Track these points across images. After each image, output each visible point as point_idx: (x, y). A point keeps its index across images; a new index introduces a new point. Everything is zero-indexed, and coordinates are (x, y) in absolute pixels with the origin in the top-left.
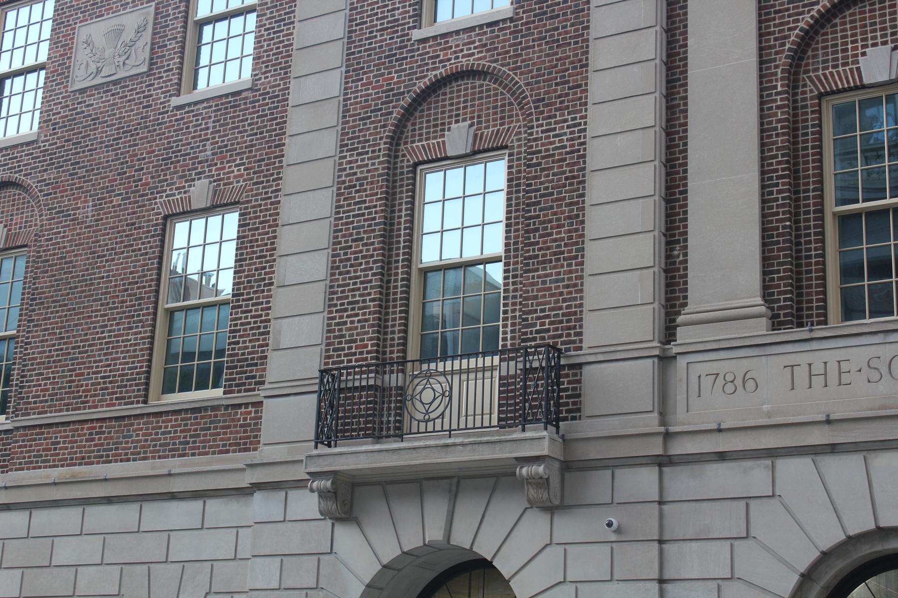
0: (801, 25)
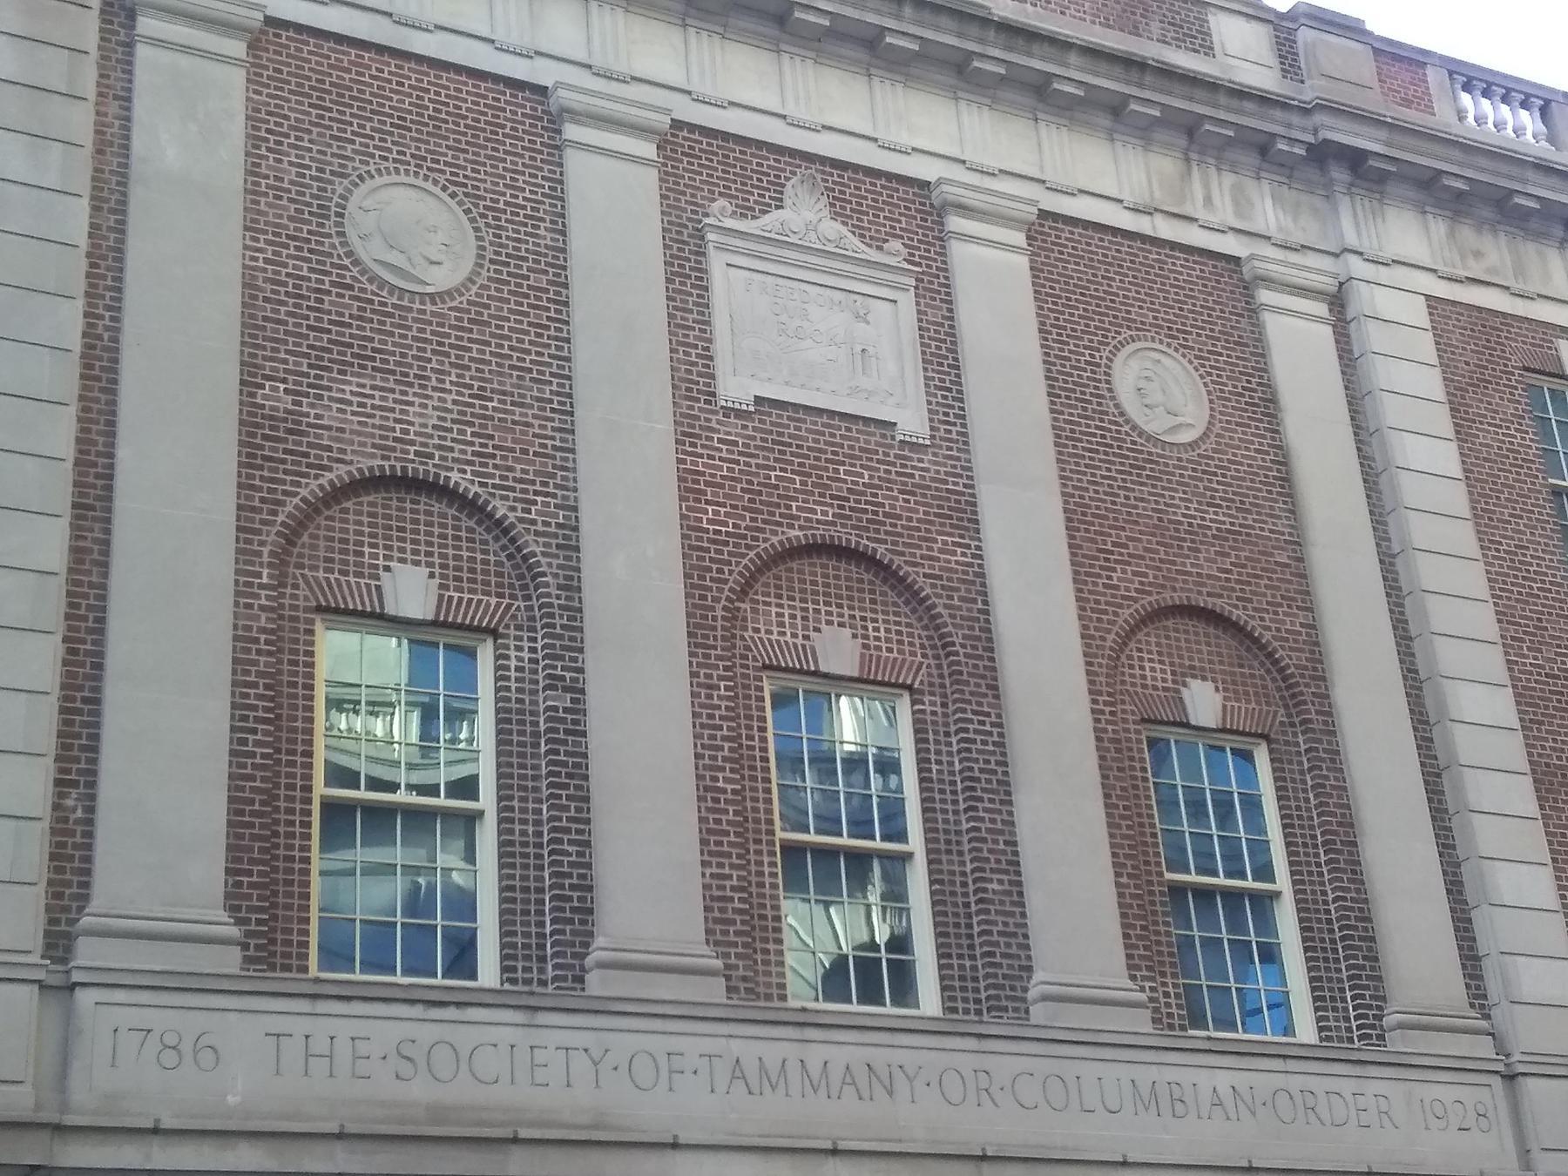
0: (304, 492)
